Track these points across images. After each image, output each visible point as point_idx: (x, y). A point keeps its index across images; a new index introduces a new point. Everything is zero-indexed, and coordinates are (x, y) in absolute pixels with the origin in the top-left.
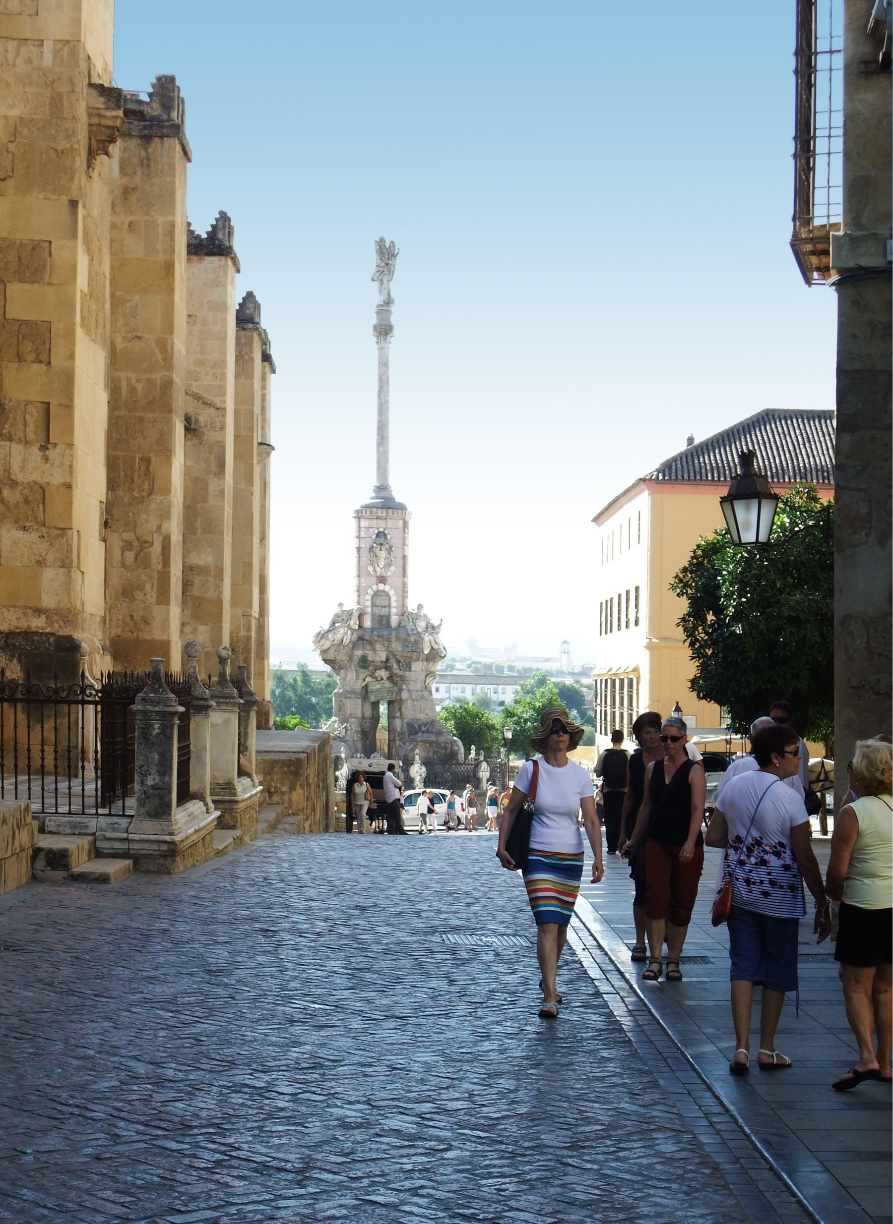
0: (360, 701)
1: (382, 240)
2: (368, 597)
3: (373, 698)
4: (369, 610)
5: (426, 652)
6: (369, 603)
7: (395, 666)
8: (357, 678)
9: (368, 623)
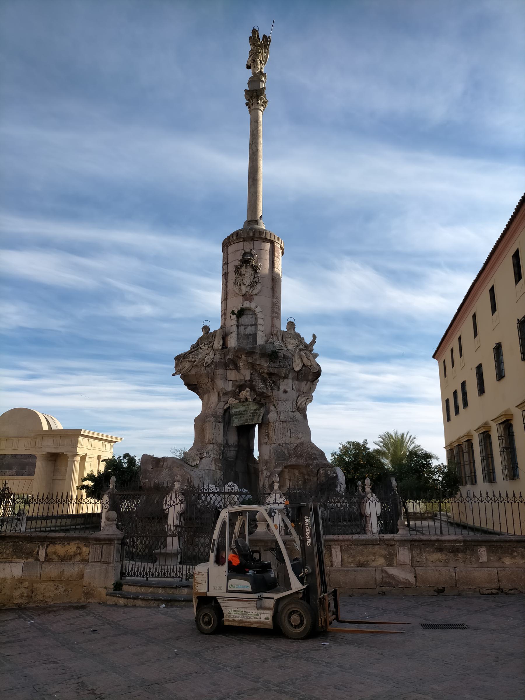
0: (221, 425)
3: (236, 422)
4: (234, 328)
5: (297, 369)
6: (234, 322)
7: (261, 385)
8: (219, 401)
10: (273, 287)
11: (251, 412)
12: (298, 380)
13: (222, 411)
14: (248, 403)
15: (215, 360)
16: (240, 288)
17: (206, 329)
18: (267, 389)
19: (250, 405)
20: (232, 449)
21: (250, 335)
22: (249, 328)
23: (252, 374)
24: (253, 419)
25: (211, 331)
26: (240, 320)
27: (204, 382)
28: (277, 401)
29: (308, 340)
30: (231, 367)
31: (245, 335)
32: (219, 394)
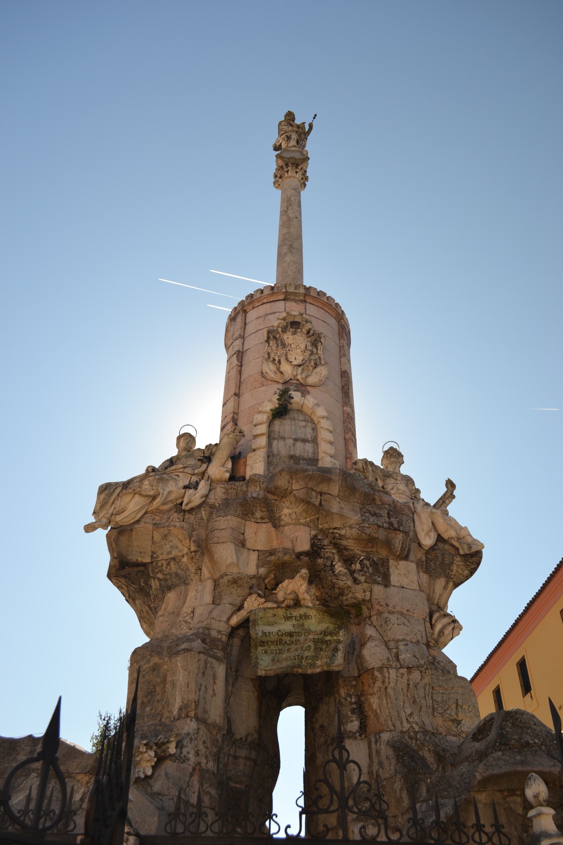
0: (221, 670)
1: (290, 116)
2: (264, 418)
4: (263, 441)
6: (263, 429)
7: (339, 567)
10: (343, 387)
11: (311, 637)
12: (427, 571)
13: (225, 628)
14: (302, 611)
15: (211, 500)
16: (278, 369)
17: (186, 440)
18: (356, 581)
19: (306, 617)
21: (304, 459)
22: (299, 445)
23: (314, 538)
24: (316, 657)
25: (201, 444)
26: (277, 422)
27: (175, 553)
28: (386, 615)
29: (431, 494)
30: (258, 514)
31: (291, 457)
32: (216, 584)
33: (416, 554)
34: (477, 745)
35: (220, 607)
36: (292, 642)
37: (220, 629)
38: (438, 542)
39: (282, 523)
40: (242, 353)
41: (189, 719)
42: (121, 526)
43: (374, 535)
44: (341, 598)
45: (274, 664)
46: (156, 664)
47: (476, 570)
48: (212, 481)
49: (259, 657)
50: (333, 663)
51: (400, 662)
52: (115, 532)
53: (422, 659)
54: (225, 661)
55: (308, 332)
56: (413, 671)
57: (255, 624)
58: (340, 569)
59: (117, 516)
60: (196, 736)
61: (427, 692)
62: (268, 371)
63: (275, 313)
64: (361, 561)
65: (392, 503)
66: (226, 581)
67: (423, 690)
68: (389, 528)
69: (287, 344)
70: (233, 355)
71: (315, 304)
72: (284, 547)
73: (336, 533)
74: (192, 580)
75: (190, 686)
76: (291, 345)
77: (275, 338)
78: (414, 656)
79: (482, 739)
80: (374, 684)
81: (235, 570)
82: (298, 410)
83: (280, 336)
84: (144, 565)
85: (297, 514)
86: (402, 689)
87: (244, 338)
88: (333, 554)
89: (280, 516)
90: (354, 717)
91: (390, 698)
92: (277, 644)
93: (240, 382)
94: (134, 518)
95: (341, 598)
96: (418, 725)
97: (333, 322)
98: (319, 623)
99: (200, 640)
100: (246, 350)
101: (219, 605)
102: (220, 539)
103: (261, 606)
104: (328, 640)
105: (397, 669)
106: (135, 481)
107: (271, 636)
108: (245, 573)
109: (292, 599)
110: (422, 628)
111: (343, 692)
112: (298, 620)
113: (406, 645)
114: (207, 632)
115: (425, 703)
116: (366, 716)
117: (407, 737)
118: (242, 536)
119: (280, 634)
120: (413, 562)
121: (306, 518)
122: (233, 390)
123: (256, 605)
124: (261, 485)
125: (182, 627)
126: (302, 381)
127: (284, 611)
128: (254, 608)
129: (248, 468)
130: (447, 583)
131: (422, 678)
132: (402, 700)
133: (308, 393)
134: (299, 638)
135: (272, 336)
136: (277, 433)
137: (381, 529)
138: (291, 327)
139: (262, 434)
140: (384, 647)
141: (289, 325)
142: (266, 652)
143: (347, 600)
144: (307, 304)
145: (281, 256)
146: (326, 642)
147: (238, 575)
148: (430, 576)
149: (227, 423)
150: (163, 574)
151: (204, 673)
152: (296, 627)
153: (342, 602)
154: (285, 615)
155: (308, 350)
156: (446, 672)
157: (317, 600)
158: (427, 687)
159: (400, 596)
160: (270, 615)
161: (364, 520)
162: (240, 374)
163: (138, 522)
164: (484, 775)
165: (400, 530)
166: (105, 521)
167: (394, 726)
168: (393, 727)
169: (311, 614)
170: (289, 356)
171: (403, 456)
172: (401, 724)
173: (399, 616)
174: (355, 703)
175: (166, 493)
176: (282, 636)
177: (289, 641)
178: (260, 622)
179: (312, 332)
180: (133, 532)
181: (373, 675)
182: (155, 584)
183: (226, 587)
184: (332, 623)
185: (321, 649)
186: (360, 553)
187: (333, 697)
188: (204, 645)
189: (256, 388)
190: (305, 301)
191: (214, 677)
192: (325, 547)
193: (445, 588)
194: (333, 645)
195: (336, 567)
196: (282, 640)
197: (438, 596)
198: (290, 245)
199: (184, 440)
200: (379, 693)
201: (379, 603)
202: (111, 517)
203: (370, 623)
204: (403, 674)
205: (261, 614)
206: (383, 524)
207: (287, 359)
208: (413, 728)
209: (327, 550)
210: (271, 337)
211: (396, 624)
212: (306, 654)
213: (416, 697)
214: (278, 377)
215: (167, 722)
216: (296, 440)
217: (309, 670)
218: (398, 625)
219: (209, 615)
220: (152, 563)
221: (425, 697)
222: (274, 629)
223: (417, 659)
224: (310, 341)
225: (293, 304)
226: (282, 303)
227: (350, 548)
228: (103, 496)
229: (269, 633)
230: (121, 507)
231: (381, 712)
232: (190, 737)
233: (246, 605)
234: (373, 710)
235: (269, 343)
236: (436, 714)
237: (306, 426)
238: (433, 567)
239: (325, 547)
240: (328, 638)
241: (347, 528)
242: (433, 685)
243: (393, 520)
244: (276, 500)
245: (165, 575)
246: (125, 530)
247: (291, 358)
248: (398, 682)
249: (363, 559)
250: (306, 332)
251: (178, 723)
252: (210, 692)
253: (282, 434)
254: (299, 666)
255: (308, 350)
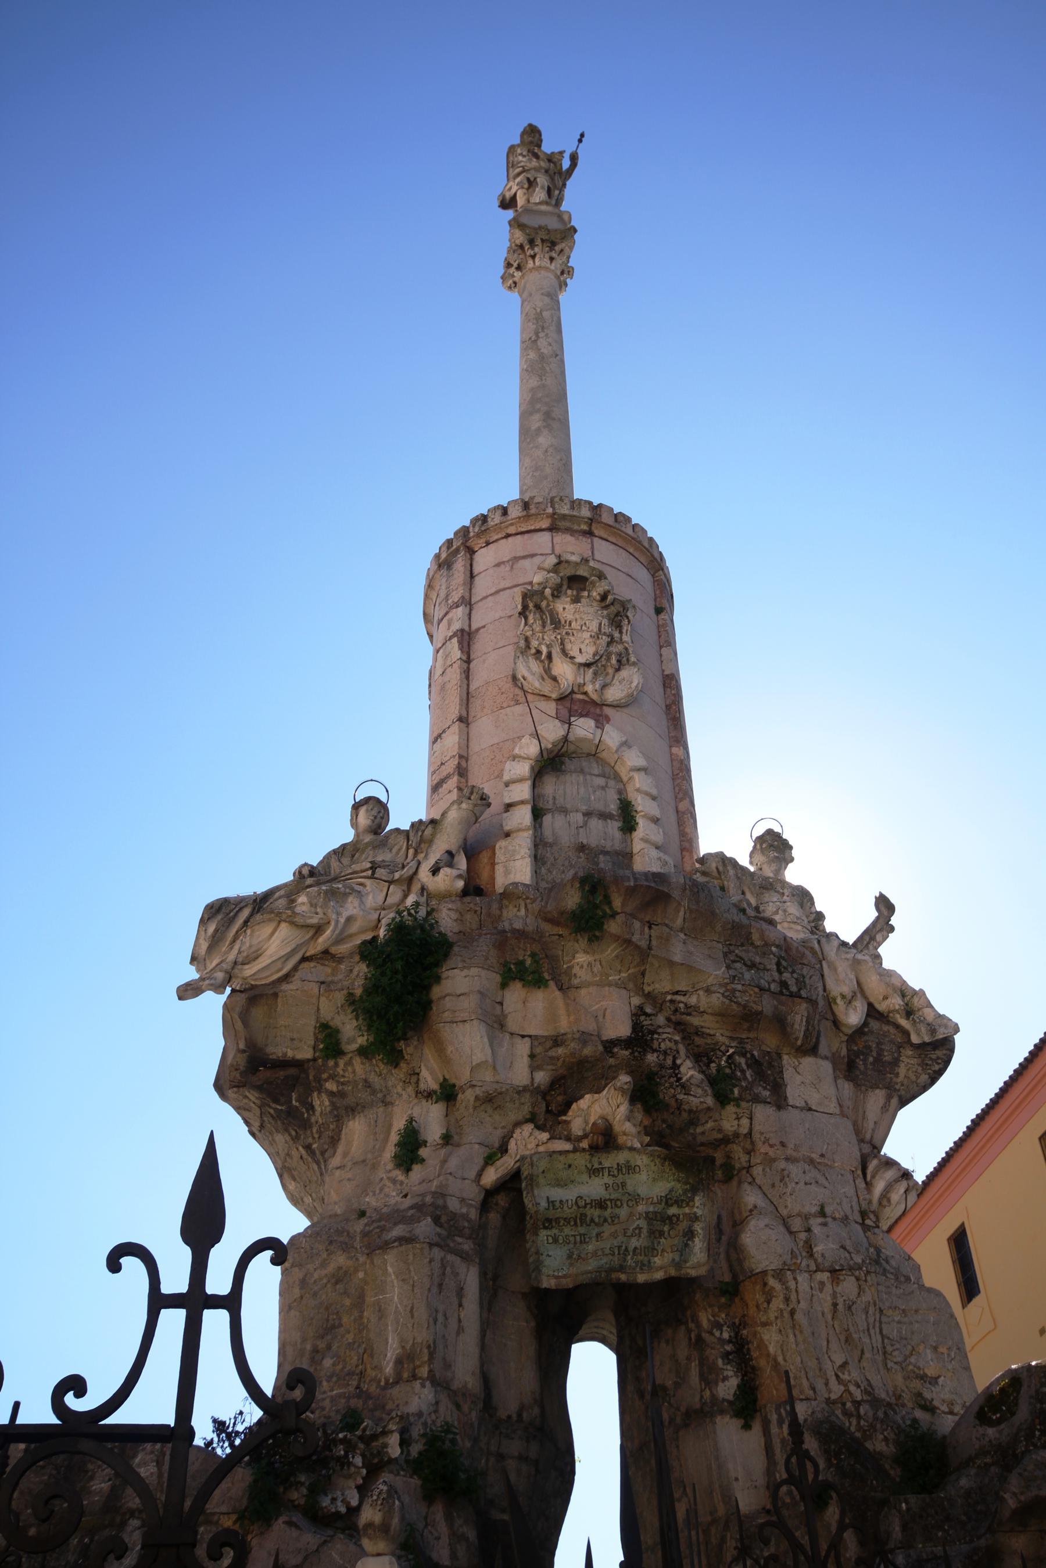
1: (532, 135)
2: (523, 769)
4: (523, 816)
6: (523, 791)
7: (688, 1071)
9: (514, 866)
10: (668, 707)
11: (641, 1208)
13: (473, 1194)
14: (622, 1157)
16: (548, 671)
17: (372, 810)
19: (630, 1168)
20: (514, 1447)
21: (606, 853)
22: (595, 823)
23: (638, 1014)
24: (651, 1250)
25: (400, 819)
29: (846, 922)
33: (831, 1043)
34: (991, 1431)
35: (462, 1151)
36: (605, 1220)
37: (465, 1195)
38: (870, 1020)
39: (575, 982)
40: (469, 634)
41: (417, 1384)
42: (253, 987)
43: (754, 1006)
44: (691, 1131)
45: (571, 1265)
46: (340, 1268)
47: (941, 1074)
48: (429, 895)
49: (542, 1250)
50: (686, 1262)
51: (816, 1261)
52: (242, 998)
53: (858, 1252)
54: (477, 1260)
55: (604, 597)
56: (842, 1278)
57: (531, 1185)
58: (691, 1072)
59: (246, 967)
60: (433, 1416)
61: (871, 1320)
62: (526, 674)
63: (532, 556)
64: (730, 1057)
65: (782, 942)
66: (472, 1099)
67: (864, 1317)
68: (781, 993)
69: (563, 622)
70: (451, 638)
71: (610, 539)
72: (582, 1029)
73: (680, 1002)
74: (400, 1095)
75: (416, 1314)
76: (570, 625)
77: (538, 607)
78: (843, 1247)
79: (999, 1422)
80: (769, 1303)
81: (488, 1076)
82: (589, 755)
83: (548, 605)
84: (299, 1064)
85: (604, 963)
86: (823, 1314)
87: (470, 604)
88: (676, 1042)
89: (571, 968)
90: (729, 1371)
91: (801, 1332)
92: (576, 1224)
93: (468, 693)
94: (280, 970)
95: (691, 1131)
96: (858, 1386)
97: (643, 575)
98: (654, 1180)
99: (429, 1219)
100: (478, 630)
101: (458, 1145)
102: (457, 1014)
103: (541, 1149)
104: (674, 1215)
105: (811, 1273)
106: (277, 894)
107: (565, 1208)
108: (509, 1082)
109: (602, 1134)
110: (850, 1190)
111: (704, 1319)
112: (613, 1176)
113: (825, 1224)
114: (440, 1202)
115: (868, 1341)
116: (754, 1368)
117: (839, 1412)
118: (498, 1007)
119: (581, 1203)
120: (826, 1058)
121: (620, 972)
122: (454, 710)
123: (531, 1146)
124: (529, 906)
125: (386, 1190)
126: (595, 697)
127: (588, 1157)
128: (528, 1153)
129: (499, 870)
130: (889, 1098)
131: (861, 1291)
132: (824, 1336)
133: (608, 719)
134: (617, 1211)
135: (533, 603)
136: (551, 802)
137: (766, 996)
138: (569, 587)
139: (522, 802)
140: (782, 1229)
141: (565, 583)
142: (555, 1240)
143: (703, 1133)
144: (596, 540)
145: (526, 435)
146: (670, 1218)
147: (496, 1086)
148: (857, 1085)
149: (448, 777)
150: (338, 1082)
151: (440, 1285)
152: (611, 1189)
153: (694, 1139)
154: (589, 1166)
155: (605, 634)
156: (902, 1279)
157: (646, 1134)
158: (871, 1310)
159: (807, 1126)
160: (561, 1166)
161: (734, 977)
162: (468, 678)
163: (286, 978)
164: (1022, 1498)
165: (800, 997)
166: (220, 976)
167: (814, 1389)
168: (811, 1392)
169: (639, 1163)
170: (568, 646)
171: (791, 848)
172: (827, 1384)
173: (807, 1167)
174: (730, 1341)
175: (342, 920)
176: (585, 1207)
177: (599, 1217)
178: (542, 1181)
179: (610, 598)
180: (279, 1000)
181: (765, 1284)
182: (321, 1103)
183: (471, 1110)
184: (679, 1181)
185: (661, 1234)
186: (727, 1043)
187: (683, 1328)
188: (438, 1230)
189: (502, 708)
190: (590, 533)
191: (460, 1292)
192: (660, 1030)
193: (885, 1108)
194: (683, 1225)
195: (683, 1069)
196: (586, 1216)
197: (871, 1125)
198: (545, 414)
199: (367, 810)
200: (778, 1321)
201: (766, 1141)
202: (233, 968)
203: (750, 1180)
204: (822, 1284)
205: (543, 1165)
206: (769, 984)
207: (564, 652)
208: (850, 1394)
209: (665, 1036)
210: (531, 605)
211: (802, 1184)
212: (634, 1243)
213: (852, 1329)
214: (547, 688)
215: (373, 1389)
216: (588, 814)
217: (639, 1275)
218: (806, 1184)
219: (442, 1167)
220: (315, 1060)
221: (868, 1330)
222: (569, 1194)
223: (849, 1253)
224: (608, 615)
225: (568, 538)
226: (546, 536)
227: (708, 1031)
228: (212, 928)
229: (561, 1201)
230: (253, 949)
231: (785, 1360)
232: (422, 1420)
233: (512, 1145)
234: (768, 1355)
235: (526, 618)
236: (890, 1364)
237: (606, 786)
238: (862, 1067)
239: (660, 1030)
240: (673, 1210)
241: (701, 993)
242: (881, 1305)
243: (786, 976)
244: (560, 936)
245: (343, 1084)
246: (261, 996)
247: (574, 652)
248: (815, 1299)
249: (734, 1053)
250: (598, 598)
251: (395, 1391)
252: (453, 1324)
253: (560, 801)
254: (622, 1268)
255: (605, 634)
